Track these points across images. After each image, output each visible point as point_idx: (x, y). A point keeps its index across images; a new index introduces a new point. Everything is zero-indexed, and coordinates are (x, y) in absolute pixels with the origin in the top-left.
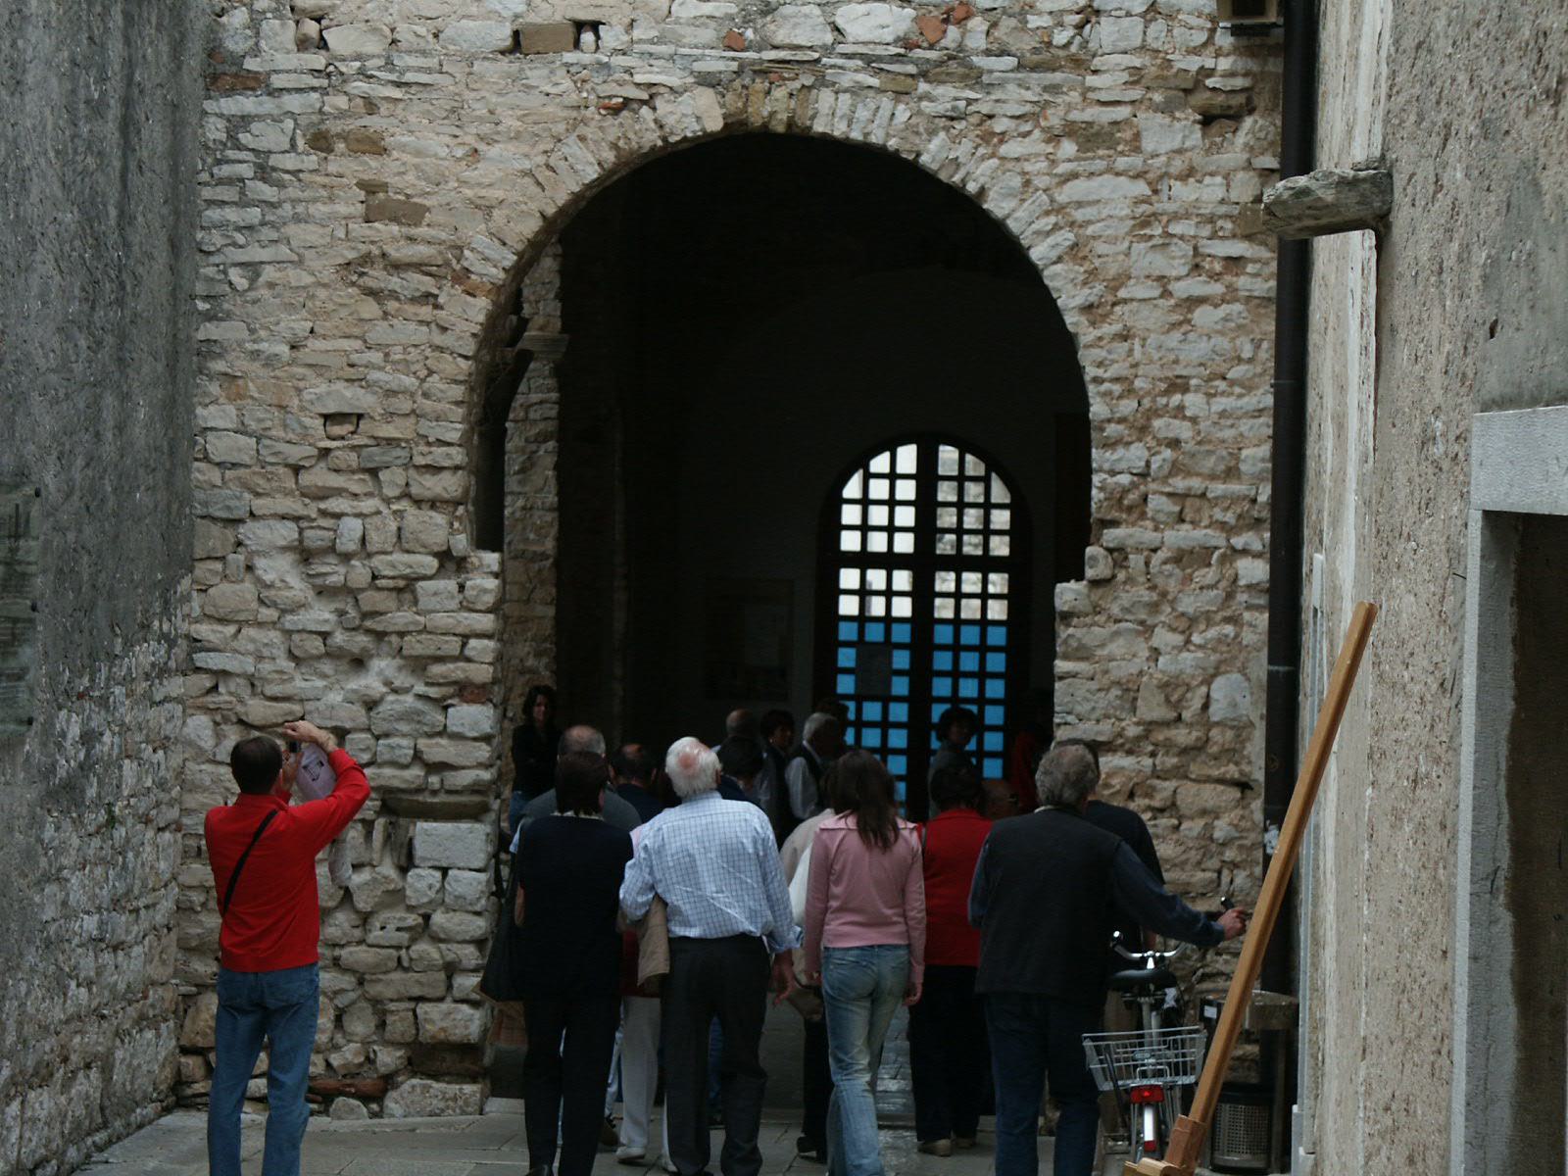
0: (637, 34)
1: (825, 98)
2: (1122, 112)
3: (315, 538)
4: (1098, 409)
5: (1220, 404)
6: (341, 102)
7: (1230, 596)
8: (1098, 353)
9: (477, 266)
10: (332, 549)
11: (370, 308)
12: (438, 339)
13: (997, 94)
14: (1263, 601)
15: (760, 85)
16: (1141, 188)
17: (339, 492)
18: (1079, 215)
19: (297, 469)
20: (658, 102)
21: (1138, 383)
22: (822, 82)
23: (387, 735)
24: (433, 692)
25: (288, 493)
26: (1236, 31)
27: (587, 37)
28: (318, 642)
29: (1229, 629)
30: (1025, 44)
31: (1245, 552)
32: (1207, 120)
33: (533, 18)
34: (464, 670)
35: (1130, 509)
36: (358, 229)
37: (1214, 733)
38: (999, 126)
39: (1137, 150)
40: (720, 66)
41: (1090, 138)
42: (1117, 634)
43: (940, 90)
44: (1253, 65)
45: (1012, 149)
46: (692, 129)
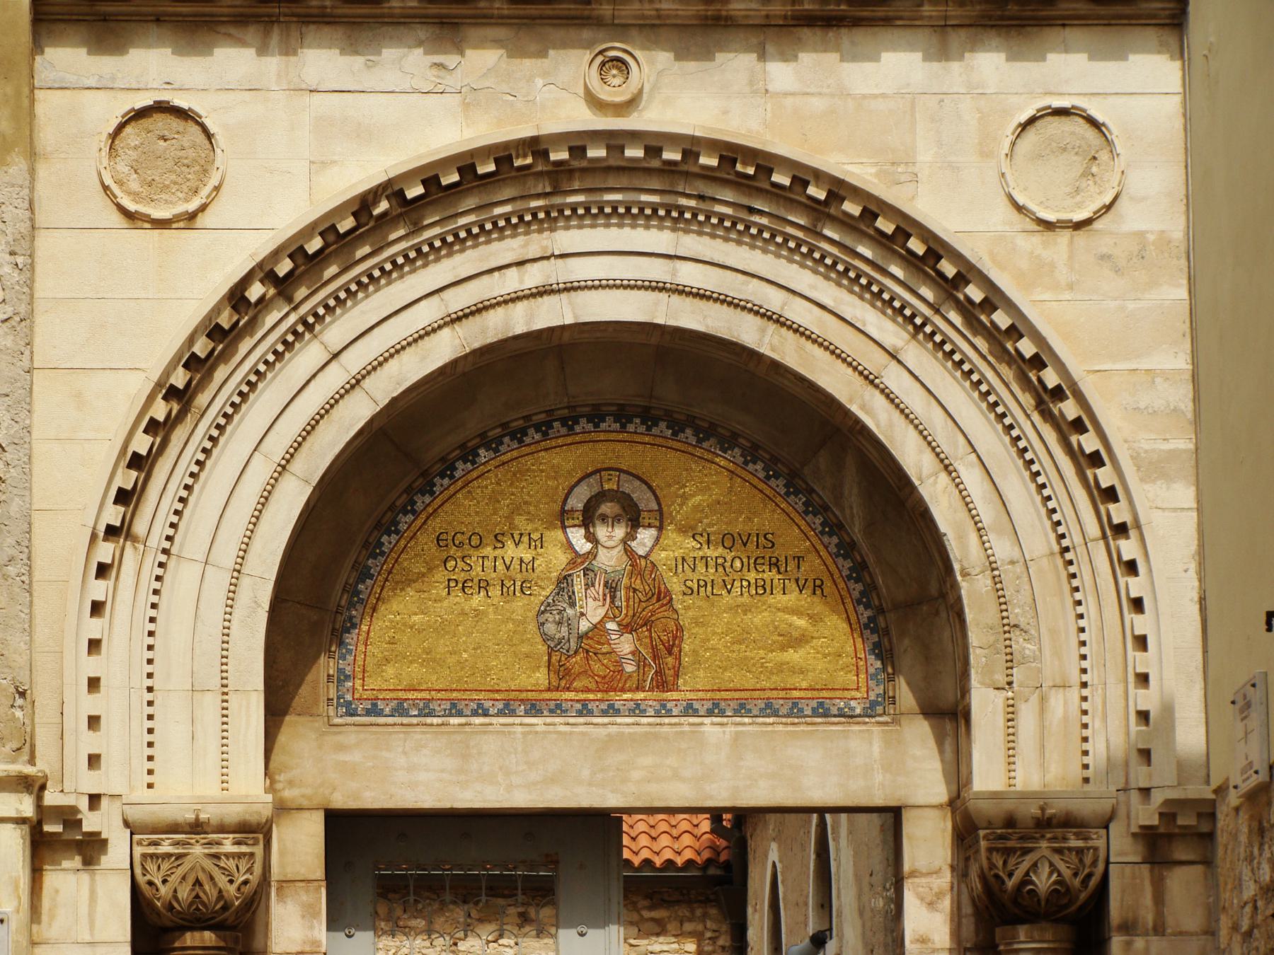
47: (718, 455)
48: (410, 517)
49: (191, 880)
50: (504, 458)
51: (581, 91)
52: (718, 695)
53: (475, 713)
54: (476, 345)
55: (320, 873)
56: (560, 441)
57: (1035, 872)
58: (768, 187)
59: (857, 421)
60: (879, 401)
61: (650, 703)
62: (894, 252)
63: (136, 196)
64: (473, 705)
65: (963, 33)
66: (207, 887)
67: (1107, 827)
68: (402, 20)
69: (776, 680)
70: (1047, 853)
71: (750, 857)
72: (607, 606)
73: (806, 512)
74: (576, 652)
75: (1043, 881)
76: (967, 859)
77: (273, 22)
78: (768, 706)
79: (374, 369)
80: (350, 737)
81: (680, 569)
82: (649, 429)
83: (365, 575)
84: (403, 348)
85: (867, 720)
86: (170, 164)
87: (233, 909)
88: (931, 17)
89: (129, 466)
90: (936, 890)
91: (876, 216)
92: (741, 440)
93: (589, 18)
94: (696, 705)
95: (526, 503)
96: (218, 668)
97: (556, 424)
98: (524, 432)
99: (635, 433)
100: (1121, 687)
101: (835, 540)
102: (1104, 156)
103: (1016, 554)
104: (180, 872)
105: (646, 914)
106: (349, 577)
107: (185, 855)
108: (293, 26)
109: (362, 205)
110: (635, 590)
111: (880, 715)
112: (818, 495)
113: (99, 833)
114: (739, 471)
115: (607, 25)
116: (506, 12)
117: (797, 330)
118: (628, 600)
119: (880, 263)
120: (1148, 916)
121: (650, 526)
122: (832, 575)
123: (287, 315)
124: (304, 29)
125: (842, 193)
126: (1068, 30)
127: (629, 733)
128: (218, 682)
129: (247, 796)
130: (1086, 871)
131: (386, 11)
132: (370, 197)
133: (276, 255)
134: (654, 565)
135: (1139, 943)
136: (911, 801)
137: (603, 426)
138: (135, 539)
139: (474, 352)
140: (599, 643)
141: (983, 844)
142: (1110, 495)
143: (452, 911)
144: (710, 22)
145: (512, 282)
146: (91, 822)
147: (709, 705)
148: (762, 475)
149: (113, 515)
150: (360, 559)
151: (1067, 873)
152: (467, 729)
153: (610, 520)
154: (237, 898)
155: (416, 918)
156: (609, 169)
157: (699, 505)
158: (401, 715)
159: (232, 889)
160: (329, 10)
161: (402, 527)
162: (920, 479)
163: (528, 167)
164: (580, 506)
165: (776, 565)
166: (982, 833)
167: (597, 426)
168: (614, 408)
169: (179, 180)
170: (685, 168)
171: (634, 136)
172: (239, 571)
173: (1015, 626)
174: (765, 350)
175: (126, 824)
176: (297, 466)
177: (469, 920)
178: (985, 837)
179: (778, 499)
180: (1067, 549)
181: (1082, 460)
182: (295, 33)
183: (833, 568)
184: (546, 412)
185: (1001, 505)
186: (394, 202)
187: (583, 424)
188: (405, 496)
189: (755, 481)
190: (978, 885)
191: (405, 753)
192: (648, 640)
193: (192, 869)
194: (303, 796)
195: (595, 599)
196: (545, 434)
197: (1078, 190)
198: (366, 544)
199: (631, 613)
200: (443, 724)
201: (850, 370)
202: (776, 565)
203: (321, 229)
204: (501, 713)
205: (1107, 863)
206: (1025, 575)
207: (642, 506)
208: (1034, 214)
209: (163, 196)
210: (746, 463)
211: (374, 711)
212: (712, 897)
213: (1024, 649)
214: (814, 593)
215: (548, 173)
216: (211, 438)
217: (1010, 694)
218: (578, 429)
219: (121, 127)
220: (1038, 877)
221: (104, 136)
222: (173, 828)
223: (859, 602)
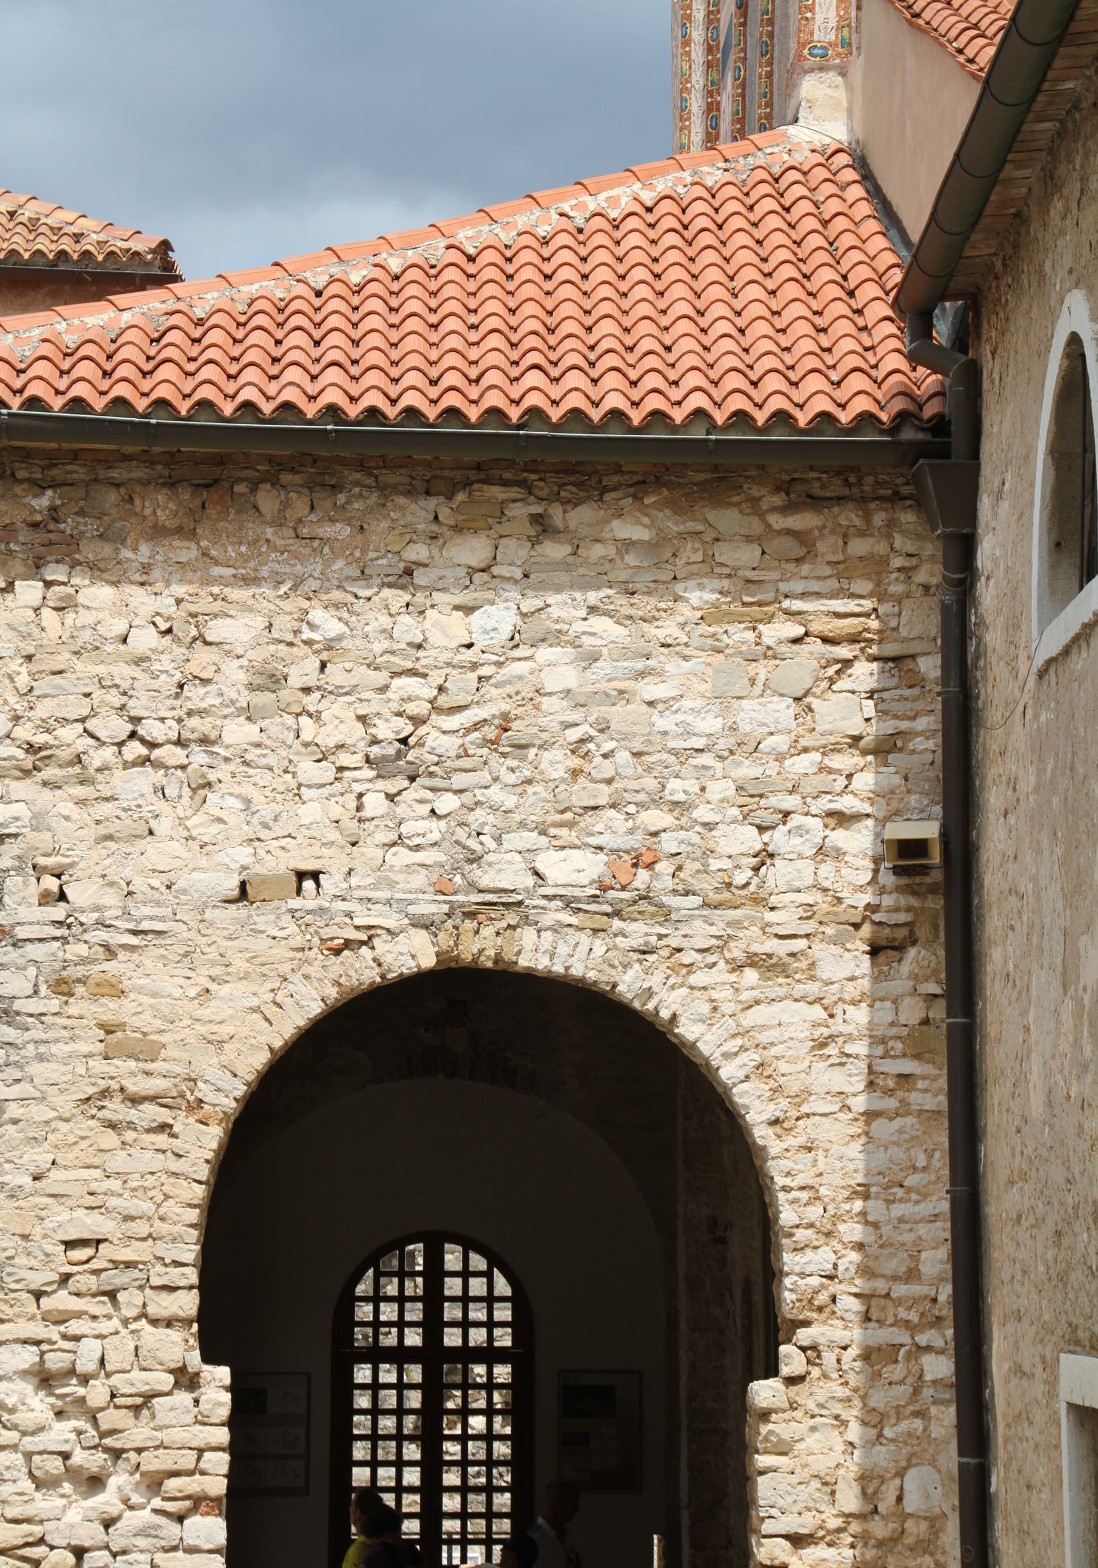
0: (354, 881)
1: (528, 935)
2: (800, 944)
3: (56, 1361)
4: (787, 1216)
5: (898, 1210)
6: (82, 950)
7: (916, 1391)
8: (785, 1164)
9: (210, 1097)
10: (72, 1372)
11: (110, 1139)
12: (175, 1165)
13: (685, 929)
14: (949, 1394)
15: (469, 925)
16: (818, 1013)
17: (79, 1315)
18: (763, 1038)
19: (38, 1295)
20: (376, 942)
21: (823, 1191)
22: (526, 920)
23: (124, 1552)
24: (171, 1507)
25: (32, 1318)
26: (897, 871)
27: (309, 885)
28: (58, 1462)
29: (918, 1424)
30: (706, 885)
31: (928, 1349)
32: (875, 951)
33: (258, 869)
34: (200, 1484)
35: (820, 1309)
36: (98, 1066)
37: (909, 1525)
38: (686, 958)
39: (812, 978)
40: (433, 908)
42: (813, 1429)
43: (634, 926)
44: (913, 901)
45: (699, 978)
46: (406, 966)
105: (777, 521)
143: (402, 509)
155: (332, 520)
177: (435, 528)
212: (905, 490)
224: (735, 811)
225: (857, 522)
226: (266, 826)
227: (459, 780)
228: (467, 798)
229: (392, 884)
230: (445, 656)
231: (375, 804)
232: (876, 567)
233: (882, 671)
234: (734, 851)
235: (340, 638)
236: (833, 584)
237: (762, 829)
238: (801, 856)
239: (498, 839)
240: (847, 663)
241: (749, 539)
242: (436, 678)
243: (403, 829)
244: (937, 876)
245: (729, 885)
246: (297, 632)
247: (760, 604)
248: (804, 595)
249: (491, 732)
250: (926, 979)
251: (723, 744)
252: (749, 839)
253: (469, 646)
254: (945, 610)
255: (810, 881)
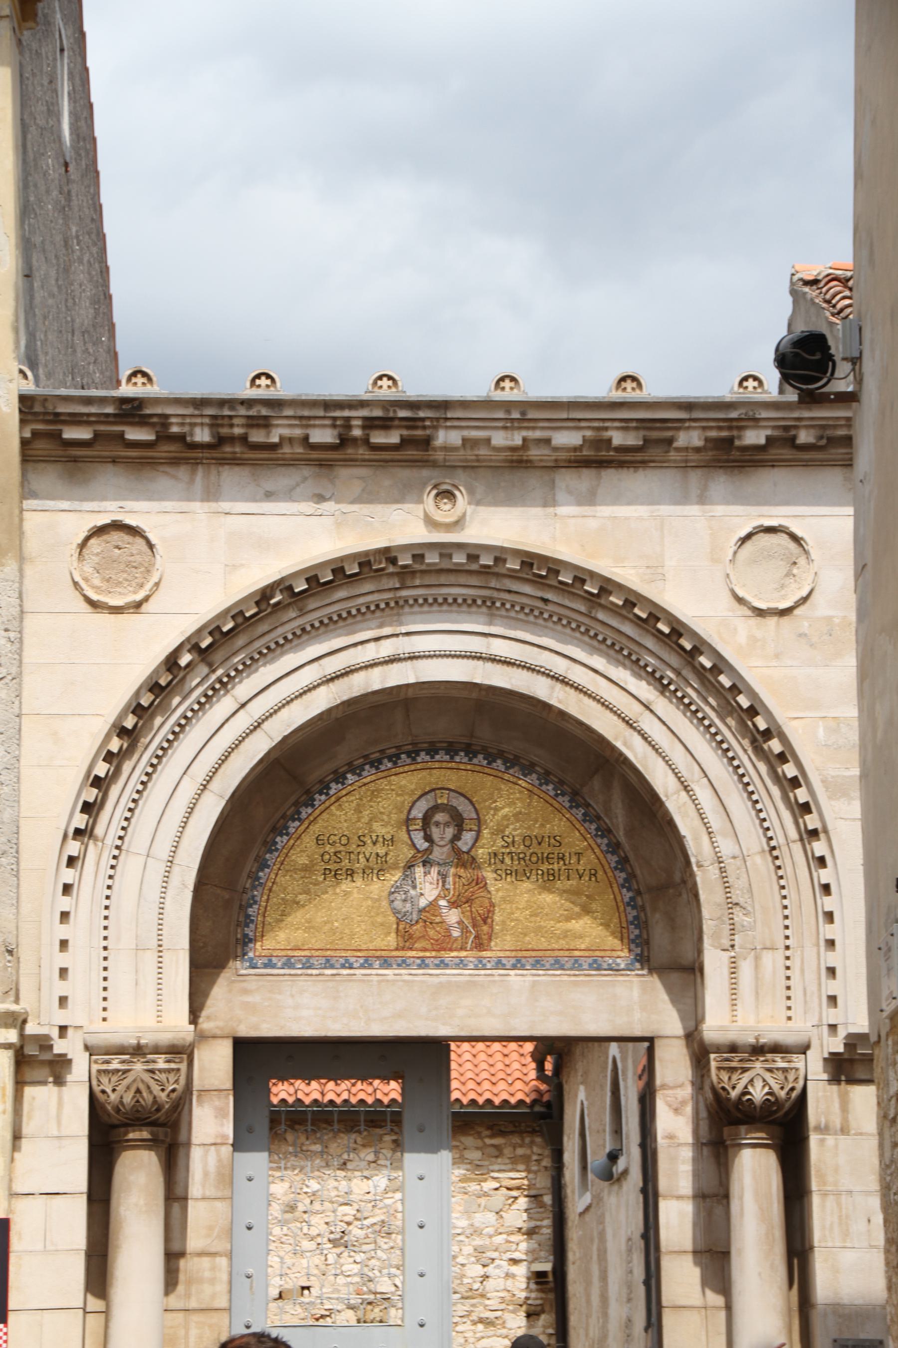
0: (324, 1290)
2: (499, 1313)
15: (369, 1307)
20: (333, 1316)
26: (537, 1283)
30: (462, 1289)
32: (529, 1316)
33: (287, 1286)
39: (504, 1327)
41: (487, 1322)
44: (543, 1295)
47: (520, 779)
48: (297, 823)
49: (133, 1089)
50: (365, 781)
51: (422, 515)
52: (520, 954)
53: (343, 967)
54: (345, 698)
55: (229, 1084)
56: (406, 768)
57: (752, 1085)
58: (556, 584)
59: (621, 754)
60: (637, 740)
61: (471, 959)
62: (648, 631)
63: (97, 589)
64: (342, 961)
65: (699, 472)
66: (145, 1094)
67: (805, 1053)
68: (292, 462)
69: (563, 943)
70: (761, 1072)
71: (566, 1097)
72: (440, 888)
73: (584, 821)
74: (417, 922)
75: (758, 1094)
76: (703, 1076)
77: (198, 464)
78: (557, 962)
79: (271, 715)
80: (252, 984)
81: (493, 861)
82: (470, 759)
83: (264, 865)
84: (292, 700)
85: (629, 973)
86: (122, 566)
87: (163, 1111)
88: (675, 461)
89: (92, 785)
90: (680, 1099)
91: (634, 605)
92: (538, 769)
93: (427, 461)
94: (504, 961)
95: (381, 813)
96: (155, 932)
97: (403, 756)
98: (380, 762)
99: (460, 762)
100: (815, 949)
101: (605, 841)
102: (802, 561)
103: (737, 852)
104: (125, 1083)
105: (488, 1141)
106: (252, 867)
107: (129, 1071)
108: (213, 467)
109: (264, 596)
110: (460, 877)
111: (638, 970)
112: (593, 808)
113: (65, 1055)
114: (535, 790)
115: (439, 466)
116: (367, 457)
117: (578, 688)
118: (454, 884)
119: (637, 639)
120: (836, 1121)
121: (471, 830)
122: (603, 866)
123: (207, 676)
124: (221, 469)
125: (610, 588)
126: (776, 470)
127: (456, 982)
128: (156, 943)
129: (175, 1027)
130: (790, 1086)
131: (280, 456)
132: (268, 591)
133: (199, 631)
134: (474, 859)
135: (830, 1140)
136: (662, 1033)
137: (437, 757)
138: (96, 839)
139: (343, 703)
140: (433, 915)
141: (713, 1065)
142: (806, 808)
143: (342, 1138)
144: (515, 464)
145: (370, 652)
146: (59, 1047)
147: (513, 961)
148: (552, 793)
149: (80, 820)
150: (261, 854)
151: (776, 1088)
152: (337, 978)
153: (442, 826)
154: (167, 1102)
155: (315, 1143)
156: (441, 571)
157: (506, 816)
158: (289, 968)
159: (163, 1096)
160: (238, 455)
161: (292, 830)
162: (667, 796)
163: (382, 569)
164: (420, 815)
165: (562, 859)
166: (712, 1056)
167: (432, 757)
168: (445, 745)
169: (129, 578)
170: (496, 570)
171: (460, 546)
172: (171, 862)
173: (737, 904)
174: (553, 702)
175: (87, 1048)
176: (214, 785)
177: (355, 1146)
178: (715, 1059)
179: (564, 811)
180: (774, 848)
181: (785, 783)
182: (213, 470)
183: (604, 861)
184: (396, 747)
185: (725, 816)
186: (285, 594)
187: (423, 756)
188: (293, 808)
189: (548, 798)
190: (709, 1095)
191: (292, 996)
192: (469, 914)
193: (134, 1081)
194: (217, 1028)
195: (431, 883)
196: (395, 763)
197: (783, 586)
198: (265, 843)
199: (457, 894)
200: (319, 975)
201: (615, 718)
202: (562, 859)
203: (233, 613)
204: (362, 967)
205: (806, 1080)
206: (744, 866)
207: (465, 815)
208: (750, 603)
209: (118, 589)
210: (541, 785)
211: (269, 965)
212: (537, 1129)
213: (743, 920)
214: (590, 880)
215: (398, 574)
216: (152, 765)
217: (733, 954)
218: (419, 759)
219: (87, 539)
220: (755, 1089)
221: (74, 546)
222: (120, 1050)
223: (623, 886)
224: (473, 1259)
225: (519, 1141)
226: (289, 1268)
227: (365, 1248)
228: (368, 1255)
229: (338, 1291)
230: (360, 1197)
231: (331, 1258)
232: (526, 1159)
233: (530, 1202)
234: (473, 1275)
235: (318, 1191)
236: (510, 1166)
237: (484, 1266)
238: (499, 1277)
239: (380, 1272)
240: (516, 1198)
241: (477, 1148)
242: (356, 1206)
243: (344, 1268)
244: (552, 1285)
245: (471, 1289)
246: (301, 1189)
247: (482, 1174)
248: (499, 1171)
249: (377, 1228)
250: (549, 1327)
251: (468, 1232)
252: (479, 1270)
253: (368, 1193)
254: (553, 1178)
255: (502, 1287)
